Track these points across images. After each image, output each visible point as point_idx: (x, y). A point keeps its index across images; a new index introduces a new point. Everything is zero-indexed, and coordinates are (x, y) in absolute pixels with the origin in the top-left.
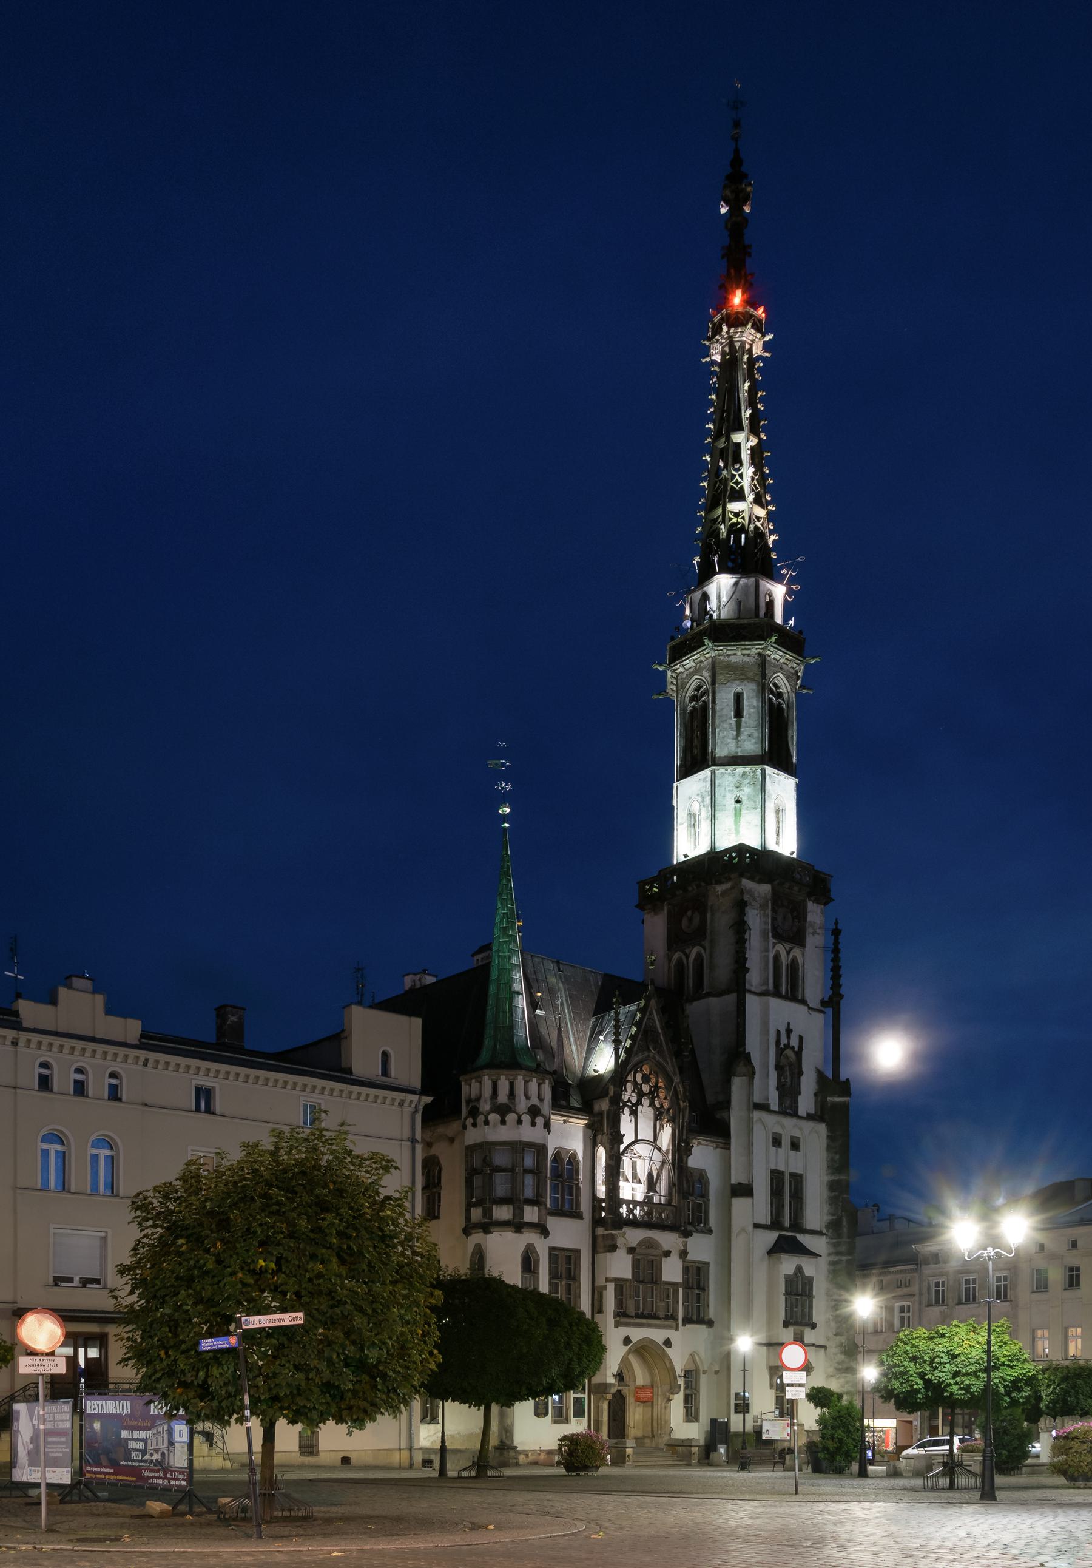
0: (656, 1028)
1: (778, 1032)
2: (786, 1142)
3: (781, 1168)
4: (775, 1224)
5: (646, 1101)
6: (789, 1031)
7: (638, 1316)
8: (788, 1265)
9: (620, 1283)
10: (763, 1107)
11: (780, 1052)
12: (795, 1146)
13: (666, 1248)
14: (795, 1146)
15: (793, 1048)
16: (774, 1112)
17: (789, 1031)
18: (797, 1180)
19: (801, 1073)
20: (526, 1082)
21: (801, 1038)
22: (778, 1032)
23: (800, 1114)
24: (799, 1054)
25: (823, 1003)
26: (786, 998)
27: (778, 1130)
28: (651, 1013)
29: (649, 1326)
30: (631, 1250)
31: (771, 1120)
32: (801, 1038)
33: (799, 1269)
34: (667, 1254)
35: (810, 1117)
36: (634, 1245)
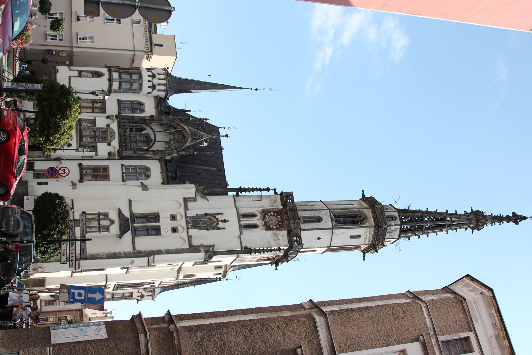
1: (222, 214)
2: (174, 224)
3: (161, 220)
4: (134, 217)
5: (172, 137)
6: (224, 221)
7: (80, 130)
8: (114, 216)
9: (94, 122)
10: (186, 208)
11: (214, 215)
12: (175, 230)
13: (112, 143)
14: (175, 230)
15: (218, 224)
16: (186, 213)
17: (224, 221)
18: (157, 231)
19: (208, 229)
20: (164, 85)
21: (224, 228)
22: (222, 214)
23: (189, 230)
24: (216, 228)
25: (246, 248)
26: (239, 221)
27: (179, 217)
28: (207, 136)
29: (77, 136)
30: (108, 126)
31: (182, 210)
32: (224, 228)
33: (112, 222)
34: (109, 144)
35: (190, 237)
36: (111, 126)
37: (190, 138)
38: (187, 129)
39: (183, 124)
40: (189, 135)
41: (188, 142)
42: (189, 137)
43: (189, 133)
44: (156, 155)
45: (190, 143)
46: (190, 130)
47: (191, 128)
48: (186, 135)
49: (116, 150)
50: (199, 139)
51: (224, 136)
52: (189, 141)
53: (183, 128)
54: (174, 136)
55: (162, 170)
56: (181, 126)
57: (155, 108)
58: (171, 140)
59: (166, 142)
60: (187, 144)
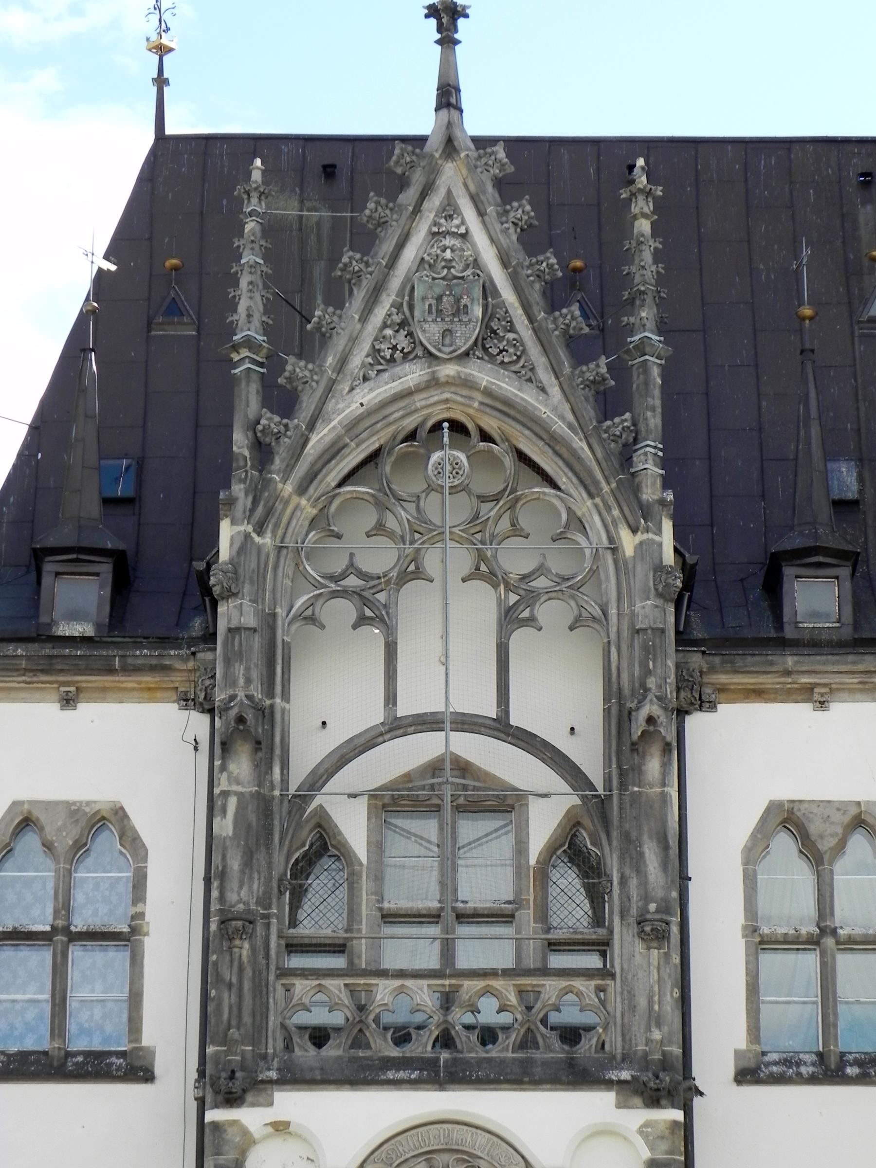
0: (476, 263)
28: (450, 210)
37: (483, 374)
38: (369, 395)
39: (312, 426)
40: (434, 383)
41: (527, 396)
42: (468, 383)
43: (413, 374)
44: (643, 734)
45: (530, 378)
46: (383, 361)
47: (359, 358)
48: (433, 407)
49: (638, 1116)
50: (489, 290)
51: (448, 40)
52: (507, 386)
53: (353, 427)
54: (438, 535)
55: (806, 694)
56: (334, 451)
57: (68, 702)
58: (484, 571)
59: (510, 620)
60: (550, 403)
